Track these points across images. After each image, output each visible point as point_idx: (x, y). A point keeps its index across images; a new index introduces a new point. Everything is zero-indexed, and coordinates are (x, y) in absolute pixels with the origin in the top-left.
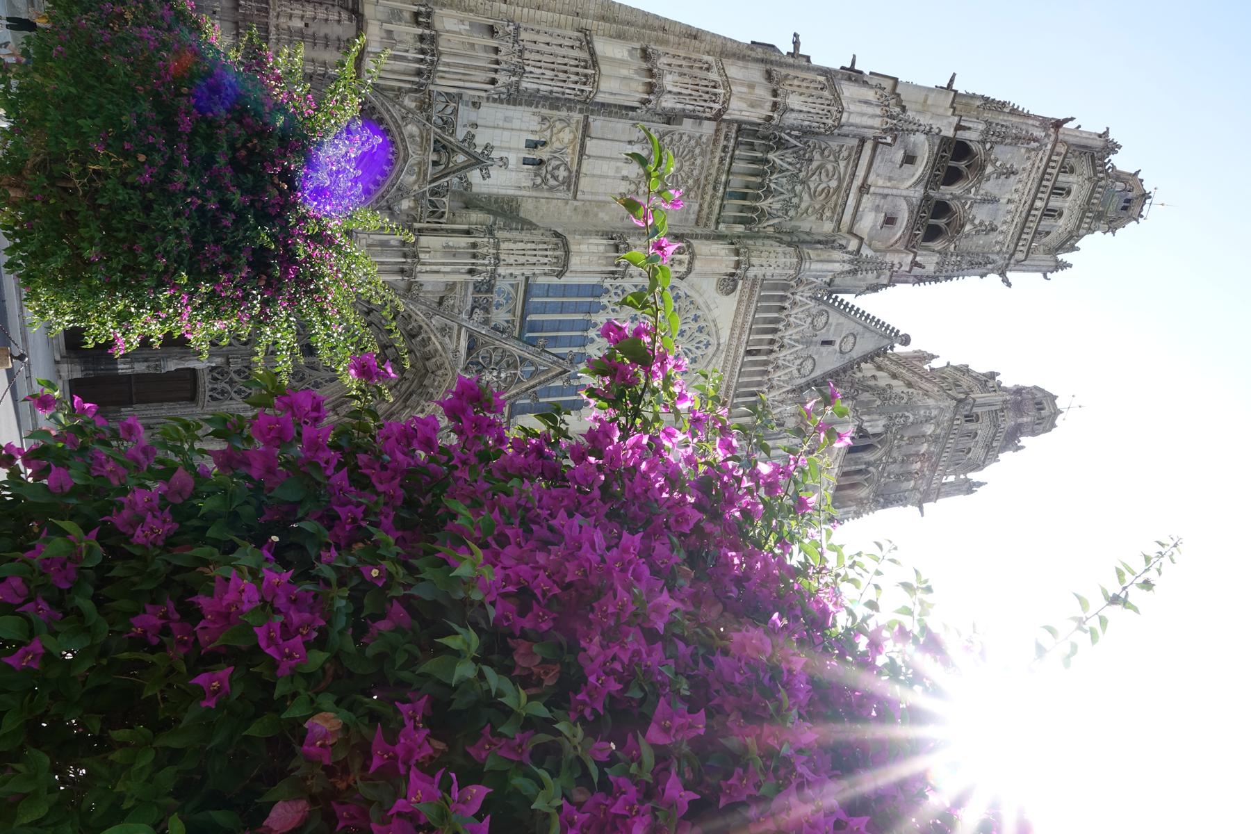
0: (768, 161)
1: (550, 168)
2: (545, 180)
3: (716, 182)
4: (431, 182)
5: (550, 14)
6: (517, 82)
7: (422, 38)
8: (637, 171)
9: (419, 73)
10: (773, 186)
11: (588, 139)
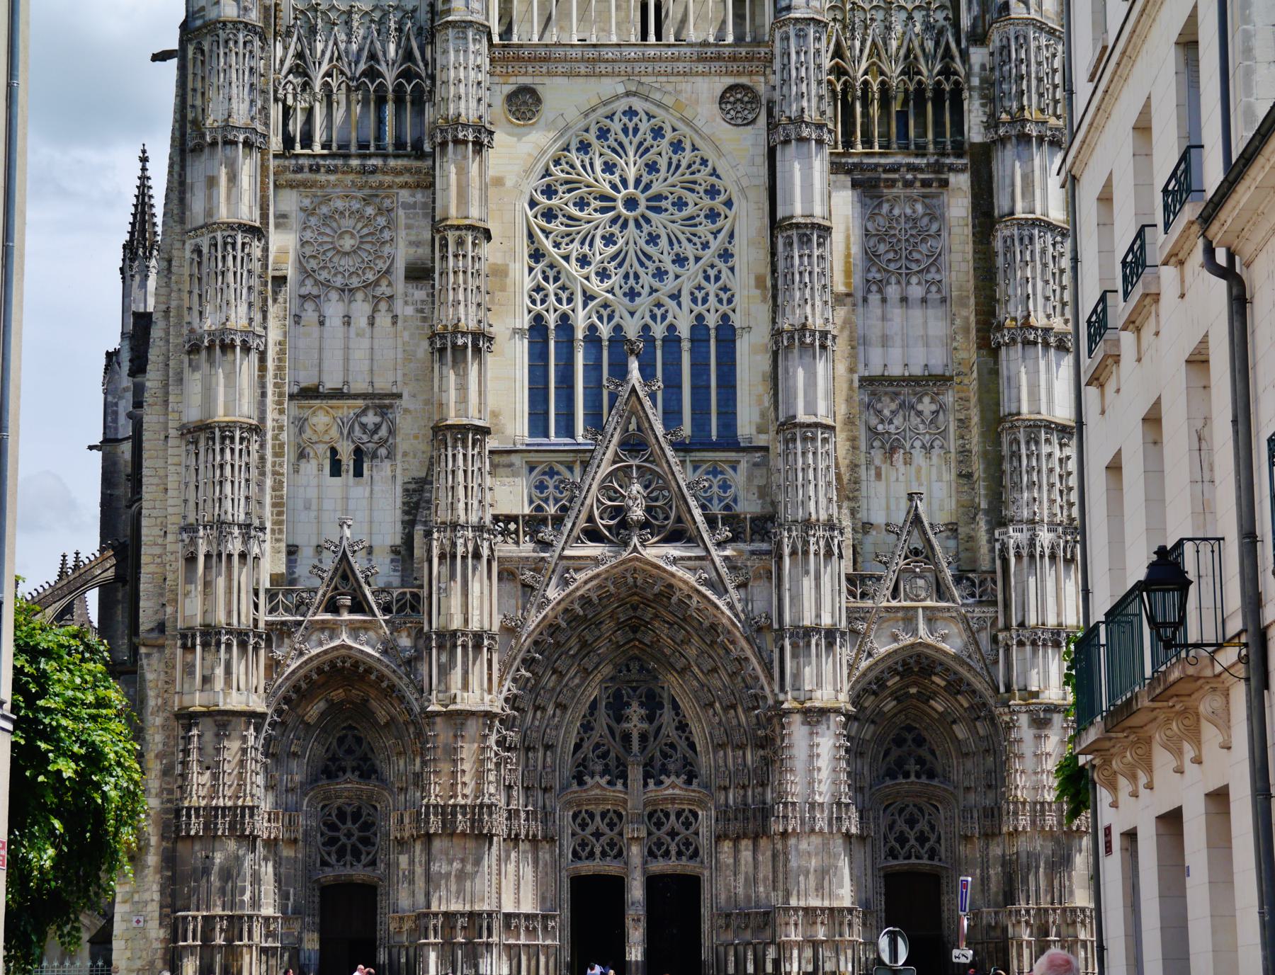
0: (326, 84)
1: (365, 438)
2: (382, 442)
3: (363, 171)
4: (374, 615)
5: (170, 479)
6: (240, 526)
7: (205, 645)
8: (359, 302)
9: (243, 645)
10: (362, 66)
11: (321, 389)
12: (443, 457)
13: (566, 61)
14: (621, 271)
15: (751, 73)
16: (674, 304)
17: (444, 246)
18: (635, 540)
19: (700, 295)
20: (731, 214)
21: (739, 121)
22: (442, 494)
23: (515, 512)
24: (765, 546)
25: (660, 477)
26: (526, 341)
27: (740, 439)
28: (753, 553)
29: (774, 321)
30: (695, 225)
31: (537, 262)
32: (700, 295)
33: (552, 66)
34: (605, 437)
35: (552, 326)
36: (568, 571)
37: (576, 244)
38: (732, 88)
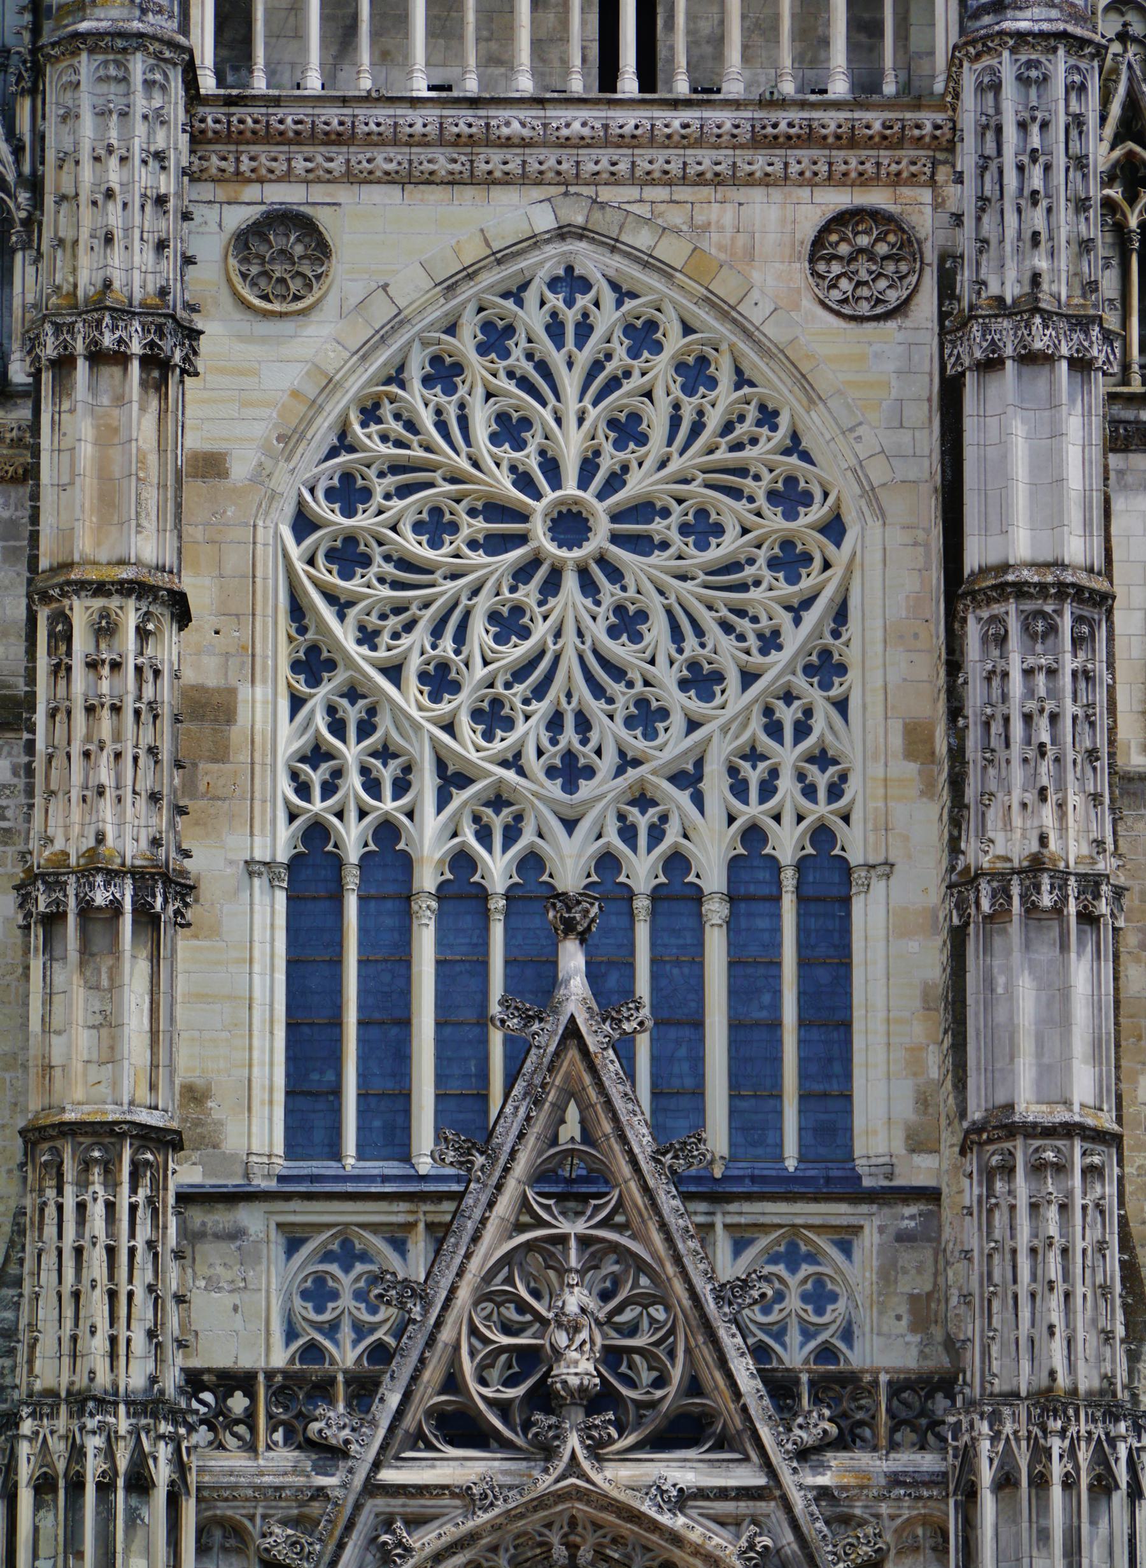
12: (51, 1211)
13: (395, 143)
14: (541, 708)
15: (896, 180)
16: (683, 798)
17: (62, 637)
18: (573, 1441)
19: (754, 775)
20: (840, 556)
21: (864, 308)
22: (46, 1312)
23: (247, 1361)
24: (928, 1462)
25: (641, 1266)
26: (281, 897)
27: (861, 1165)
28: (896, 1480)
29: (954, 848)
30: (743, 587)
31: (314, 681)
32: (754, 775)
33: (359, 156)
34: (493, 1159)
35: (353, 854)
36: (387, 1524)
37: (420, 636)
38: (842, 220)
